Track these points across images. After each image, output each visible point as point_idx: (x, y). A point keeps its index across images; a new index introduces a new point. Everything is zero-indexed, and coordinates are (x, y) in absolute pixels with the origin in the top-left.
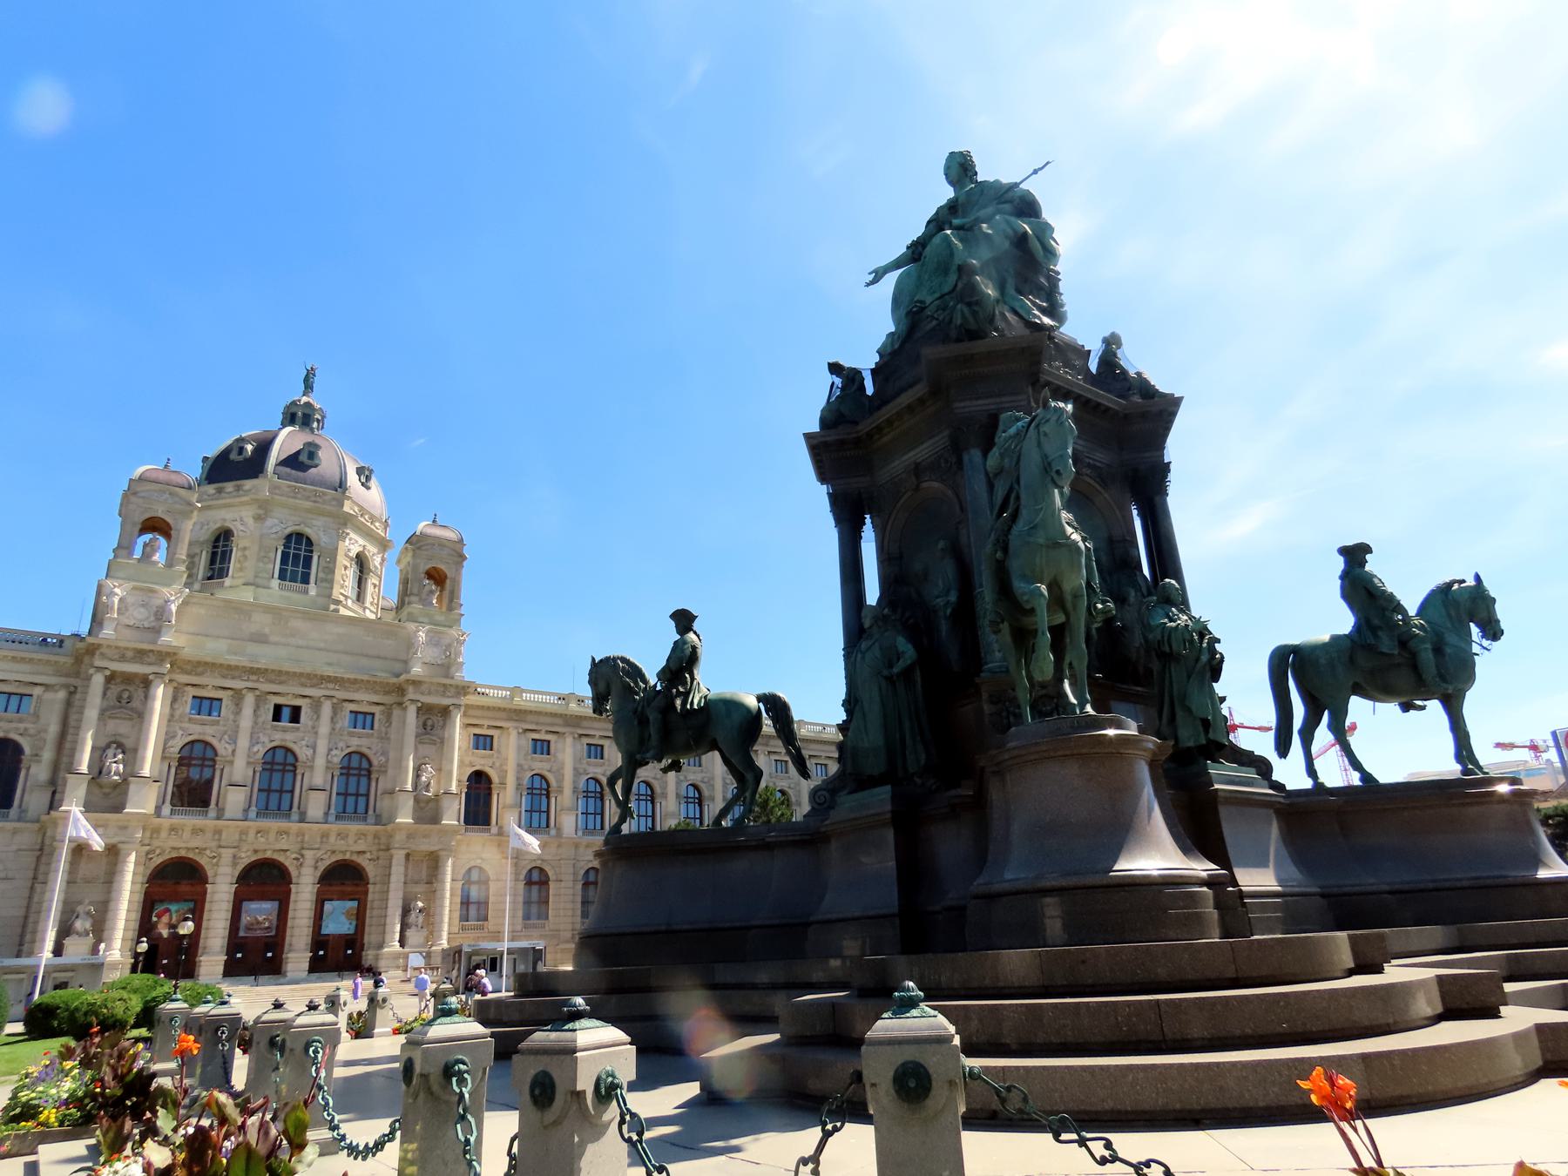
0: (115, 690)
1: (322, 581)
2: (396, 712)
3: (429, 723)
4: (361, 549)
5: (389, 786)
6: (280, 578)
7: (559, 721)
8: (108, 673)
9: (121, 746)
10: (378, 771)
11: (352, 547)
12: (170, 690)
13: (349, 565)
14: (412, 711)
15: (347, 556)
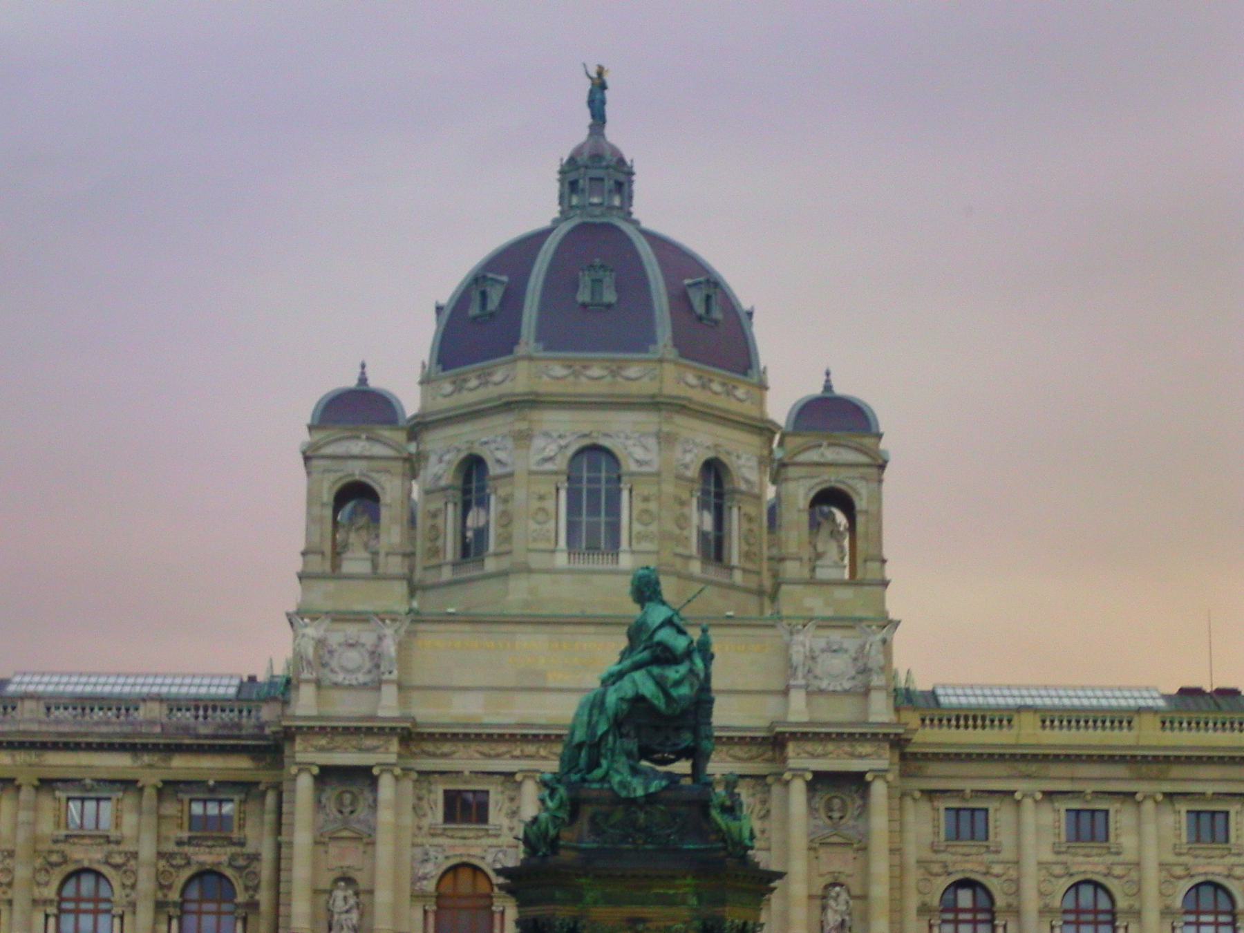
1: (639, 542)
2: (776, 789)
3: (836, 803)
4: (710, 454)
8: (316, 771)
9: (349, 881)
12: (408, 785)
13: (685, 495)
14: (798, 790)
15: (679, 477)
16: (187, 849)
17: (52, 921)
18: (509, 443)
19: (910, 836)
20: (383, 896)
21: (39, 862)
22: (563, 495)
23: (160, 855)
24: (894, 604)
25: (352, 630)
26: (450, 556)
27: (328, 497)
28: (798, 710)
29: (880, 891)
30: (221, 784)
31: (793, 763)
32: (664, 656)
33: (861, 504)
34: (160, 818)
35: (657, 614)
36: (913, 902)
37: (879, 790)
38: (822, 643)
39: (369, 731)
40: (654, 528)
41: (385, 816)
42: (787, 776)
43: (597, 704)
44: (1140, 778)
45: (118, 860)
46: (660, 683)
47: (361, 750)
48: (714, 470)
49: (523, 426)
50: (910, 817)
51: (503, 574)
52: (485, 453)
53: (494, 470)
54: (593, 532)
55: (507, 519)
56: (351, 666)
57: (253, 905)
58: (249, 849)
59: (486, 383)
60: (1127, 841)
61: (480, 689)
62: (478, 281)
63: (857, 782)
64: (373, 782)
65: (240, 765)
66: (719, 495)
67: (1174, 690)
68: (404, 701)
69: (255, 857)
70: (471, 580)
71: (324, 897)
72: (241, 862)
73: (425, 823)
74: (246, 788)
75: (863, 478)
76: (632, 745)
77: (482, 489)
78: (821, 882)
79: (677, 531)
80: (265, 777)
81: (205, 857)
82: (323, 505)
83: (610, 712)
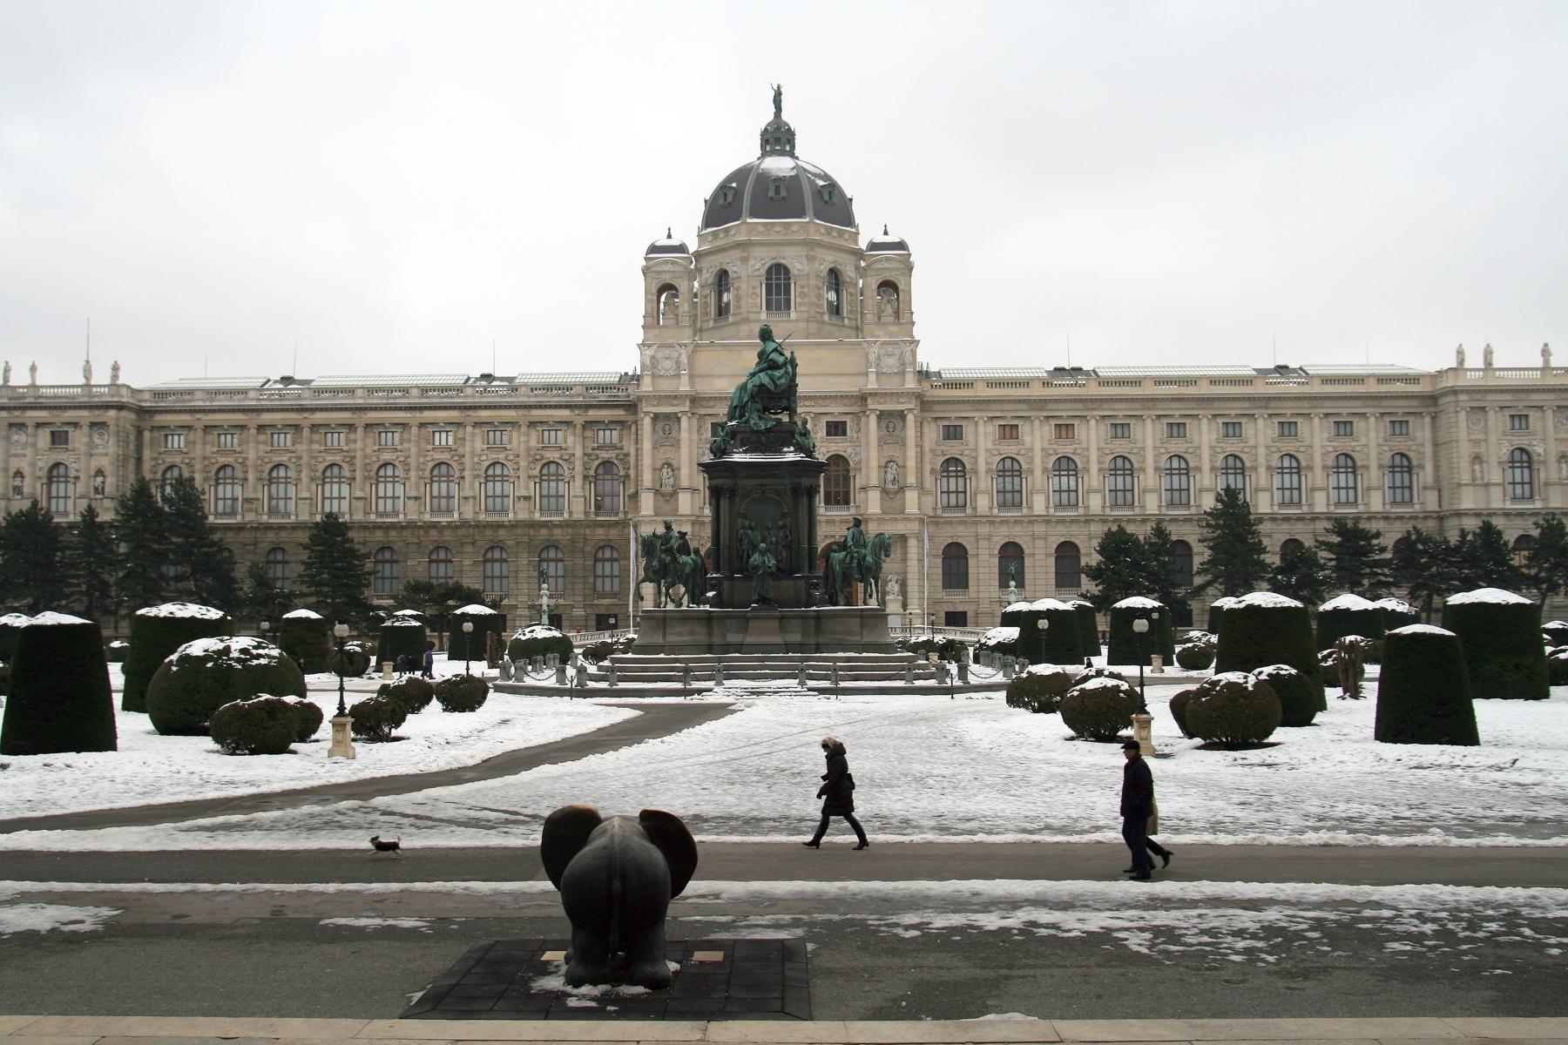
0: (659, 426)
1: (800, 305)
3: (891, 425)
4: (832, 266)
5: (864, 484)
6: (767, 309)
7: (1024, 406)
8: (652, 415)
10: (855, 469)
11: (822, 267)
12: (695, 421)
13: (820, 285)
14: (873, 419)
15: (818, 276)
16: (598, 452)
17: (538, 485)
18: (739, 263)
19: (926, 439)
20: (684, 472)
21: (531, 459)
22: (764, 286)
23: (585, 455)
24: (917, 333)
25: (667, 352)
26: (713, 315)
27: (654, 290)
28: (872, 384)
29: (911, 464)
30: (610, 422)
31: (870, 407)
32: (774, 366)
33: (901, 287)
34: (584, 438)
35: (771, 346)
36: (927, 468)
37: (910, 418)
38: (883, 352)
39: (675, 397)
40: (806, 300)
41: (684, 435)
42: (868, 413)
43: (743, 387)
44: (1033, 410)
45: (566, 457)
46: (771, 378)
47: (673, 406)
48: (834, 273)
49: (745, 254)
50: (926, 430)
51: (735, 324)
52: (730, 269)
53: (731, 275)
54: (778, 301)
55: (738, 298)
56: (667, 367)
57: (627, 476)
58: (625, 451)
59: (727, 236)
60: (1027, 438)
61: (727, 376)
62: (723, 188)
63: (901, 415)
64: (679, 419)
65: (619, 413)
66: (837, 284)
67: (1052, 369)
68: (692, 383)
69: (627, 455)
70: (723, 326)
71: (658, 472)
72: (621, 457)
73: (703, 437)
74: (621, 423)
75: (902, 275)
76: (759, 406)
77: (727, 284)
78: (883, 462)
79: (816, 301)
80: (630, 418)
81: (605, 455)
82: (652, 294)
83: (749, 392)
